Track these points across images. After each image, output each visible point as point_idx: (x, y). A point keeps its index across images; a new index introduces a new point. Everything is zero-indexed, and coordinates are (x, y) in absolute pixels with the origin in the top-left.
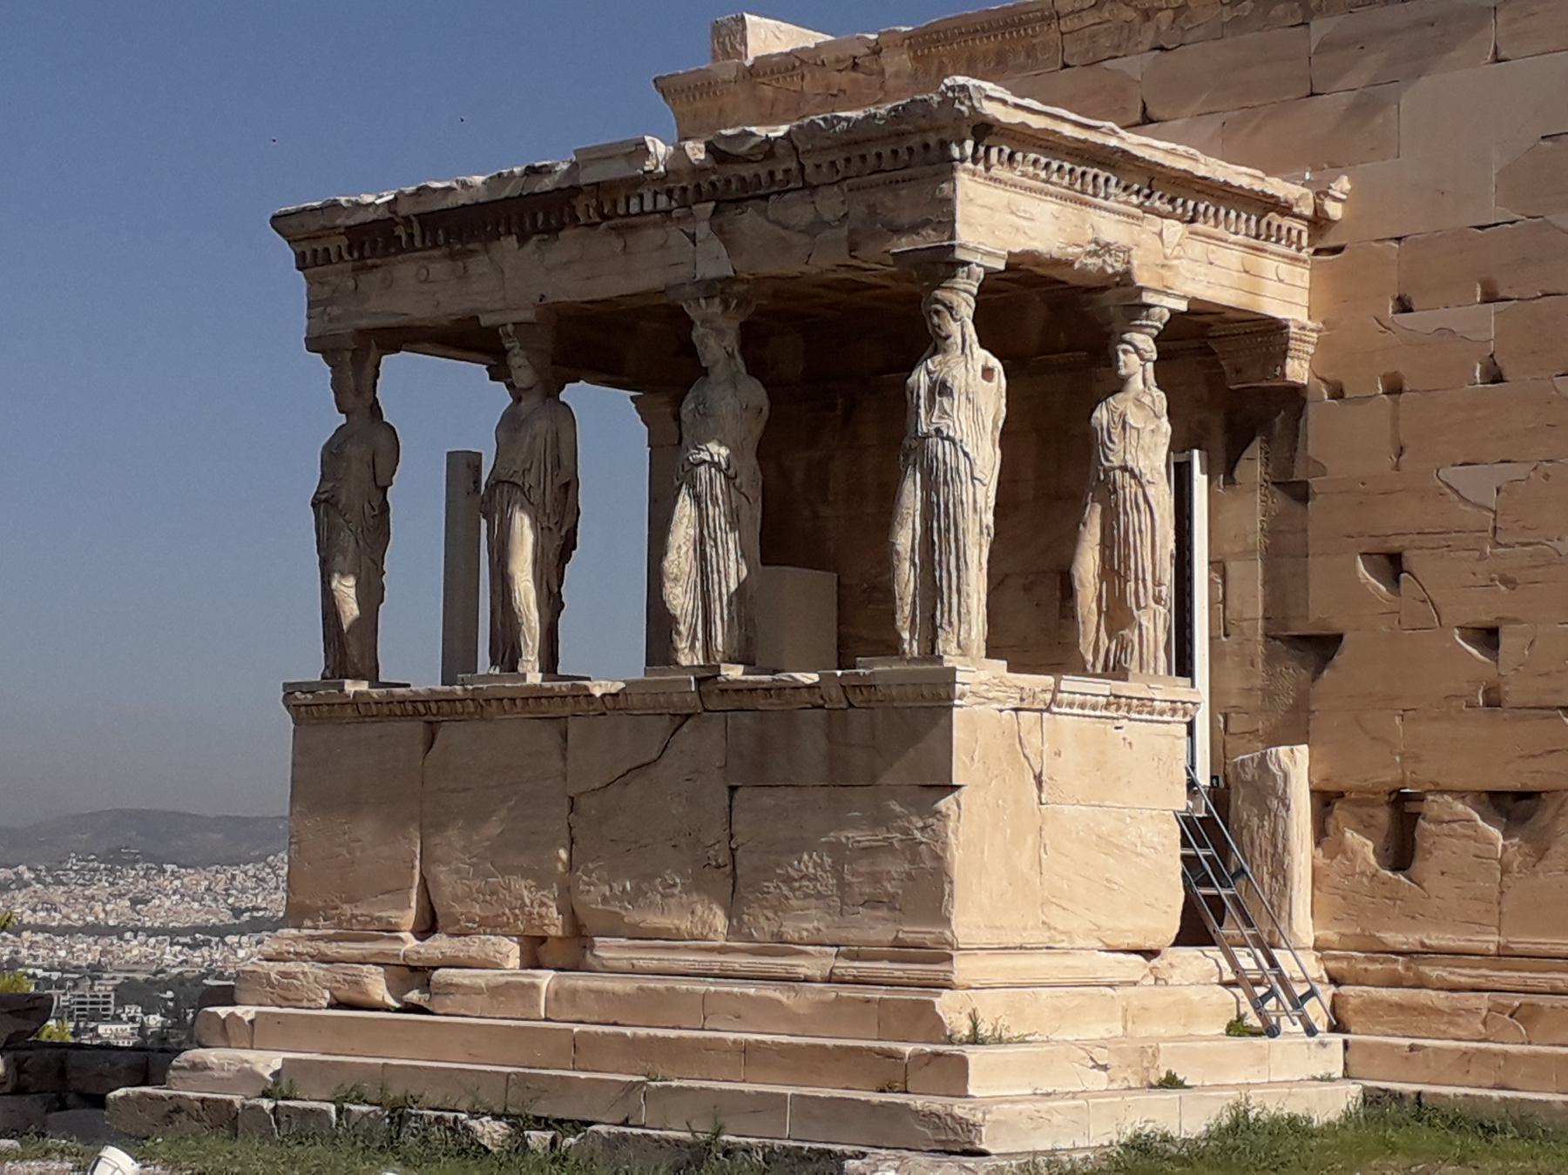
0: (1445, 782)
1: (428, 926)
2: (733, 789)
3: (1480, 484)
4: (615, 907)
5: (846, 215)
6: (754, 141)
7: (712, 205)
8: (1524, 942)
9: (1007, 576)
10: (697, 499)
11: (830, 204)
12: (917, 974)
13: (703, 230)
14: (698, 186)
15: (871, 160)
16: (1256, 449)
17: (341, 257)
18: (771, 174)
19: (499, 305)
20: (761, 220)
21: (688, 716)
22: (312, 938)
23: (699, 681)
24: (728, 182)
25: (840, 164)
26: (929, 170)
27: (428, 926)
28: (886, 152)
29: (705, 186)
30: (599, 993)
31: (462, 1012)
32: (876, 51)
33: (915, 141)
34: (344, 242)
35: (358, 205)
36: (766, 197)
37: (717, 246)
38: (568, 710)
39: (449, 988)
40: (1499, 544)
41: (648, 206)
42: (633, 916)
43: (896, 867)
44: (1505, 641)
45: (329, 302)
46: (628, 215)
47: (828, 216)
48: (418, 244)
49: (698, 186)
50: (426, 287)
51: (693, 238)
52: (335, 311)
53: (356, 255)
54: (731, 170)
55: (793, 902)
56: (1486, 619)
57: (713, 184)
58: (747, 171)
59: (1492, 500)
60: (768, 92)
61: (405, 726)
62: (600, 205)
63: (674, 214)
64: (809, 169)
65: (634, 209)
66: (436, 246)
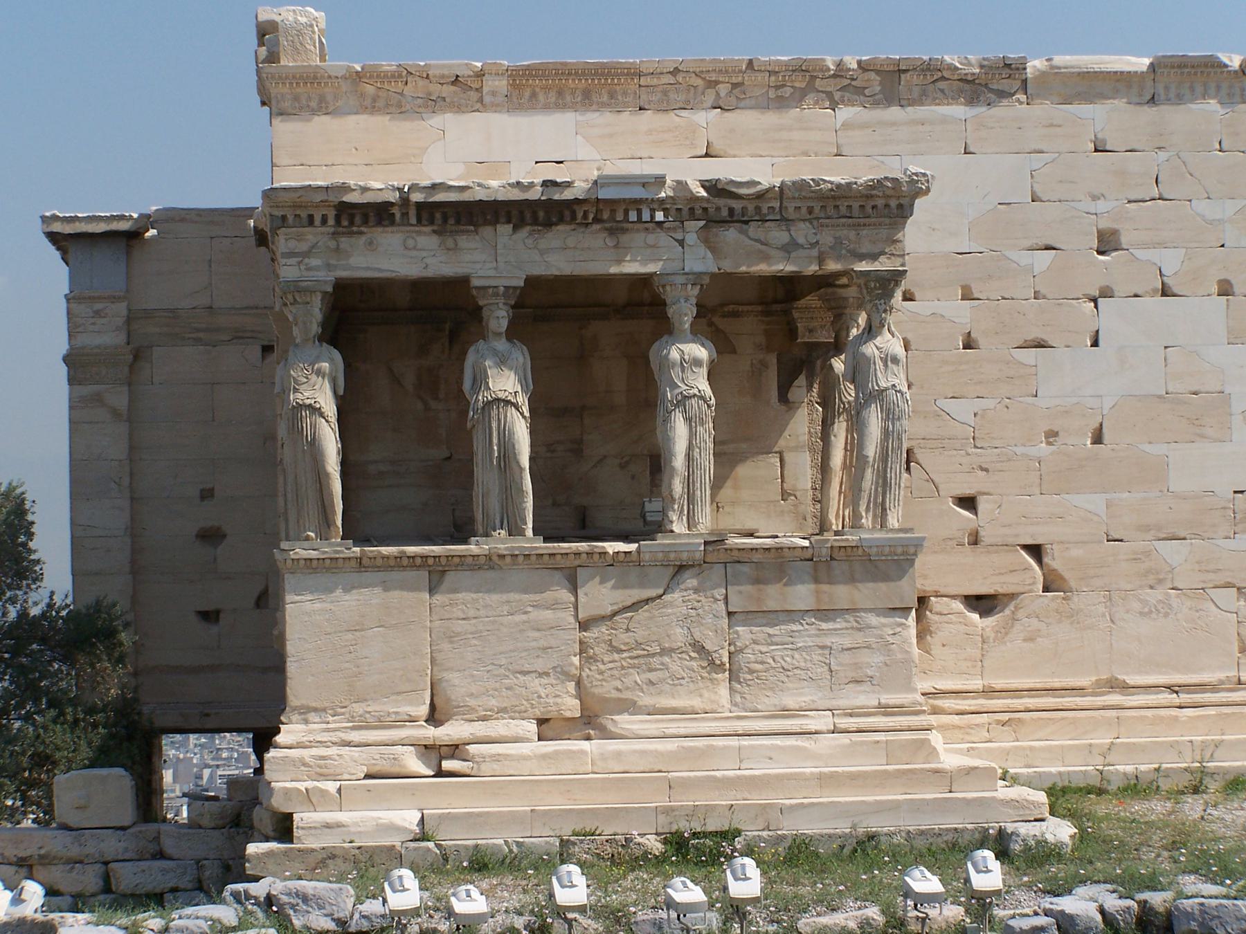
0: (943, 591)
1: (434, 717)
2: (730, 614)
3: (962, 410)
4: (627, 695)
5: (817, 242)
6: (759, 188)
7: (703, 223)
8: (999, 683)
9: (605, 457)
10: (689, 420)
11: (802, 232)
12: (906, 724)
13: (691, 238)
14: (692, 210)
15: (843, 210)
16: (802, 380)
17: (324, 220)
18: (758, 209)
19: (492, 273)
20: (742, 237)
21: (681, 568)
22: (328, 730)
23: (706, 543)
24: (718, 209)
25: (817, 209)
26: (887, 221)
27: (434, 717)
28: (856, 205)
29: (699, 212)
30: (643, 753)
31: (512, 772)
32: (480, 74)
33: (880, 202)
34: (331, 214)
35: (365, 189)
36: (746, 222)
37: (702, 250)
38: (577, 563)
39: (497, 758)
40: (976, 447)
41: (646, 216)
42: (645, 700)
43: (877, 659)
44: (982, 505)
45: (307, 254)
46: (626, 220)
47: (801, 240)
48: (413, 220)
49: (692, 210)
50: (414, 253)
51: (681, 243)
52: (315, 262)
53: (345, 223)
54: (721, 202)
55: (790, 685)
56: (967, 491)
57: (705, 209)
58: (737, 205)
59: (971, 420)
60: (370, 89)
61: (414, 573)
62: (598, 211)
63: (666, 225)
64: (791, 210)
65: (633, 216)
66: (432, 222)
